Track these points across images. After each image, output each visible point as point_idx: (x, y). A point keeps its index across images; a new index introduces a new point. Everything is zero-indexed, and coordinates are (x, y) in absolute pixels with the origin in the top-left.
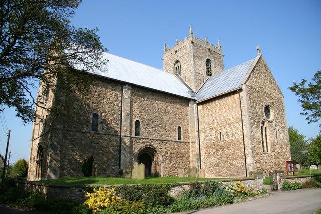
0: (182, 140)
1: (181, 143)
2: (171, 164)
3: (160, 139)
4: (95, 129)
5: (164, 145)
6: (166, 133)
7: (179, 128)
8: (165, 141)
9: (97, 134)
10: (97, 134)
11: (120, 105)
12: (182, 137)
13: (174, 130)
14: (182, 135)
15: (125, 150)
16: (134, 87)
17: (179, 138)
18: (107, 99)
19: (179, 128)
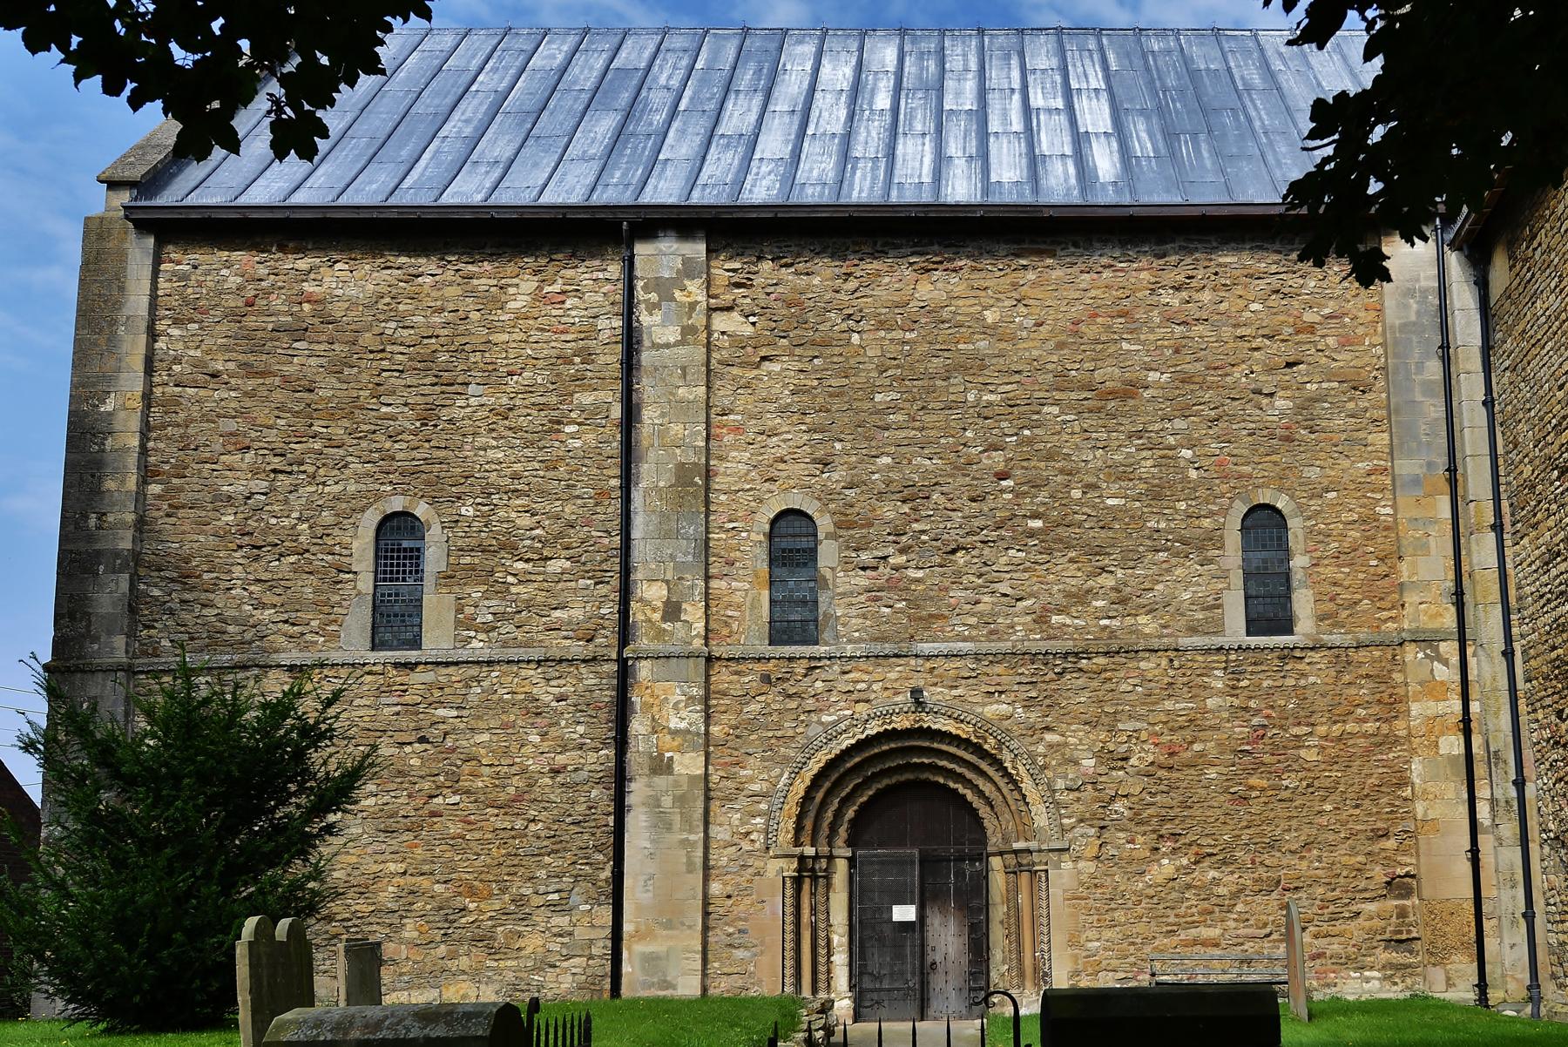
0: (1305, 625)
1: (1287, 654)
2: (1167, 866)
3: (1036, 642)
4: (395, 622)
5: (1078, 694)
6: (1107, 581)
7: (1265, 524)
8: (1085, 653)
9: (410, 666)
10: (410, 666)
11: (616, 412)
12: (1303, 604)
13: (1203, 545)
14: (1297, 577)
15: (661, 766)
16: (732, 230)
17: (1270, 613)
18: (492, 376)
19: (1265, 524)
